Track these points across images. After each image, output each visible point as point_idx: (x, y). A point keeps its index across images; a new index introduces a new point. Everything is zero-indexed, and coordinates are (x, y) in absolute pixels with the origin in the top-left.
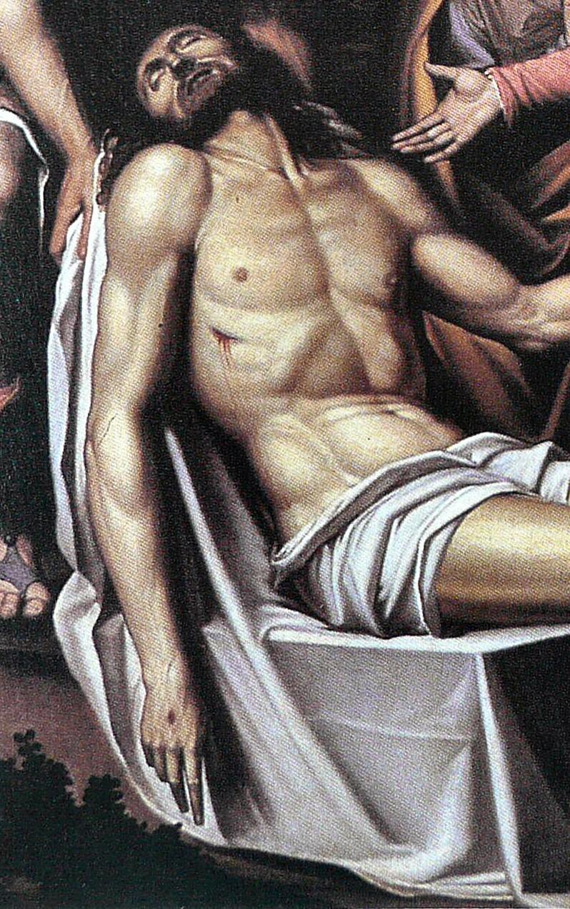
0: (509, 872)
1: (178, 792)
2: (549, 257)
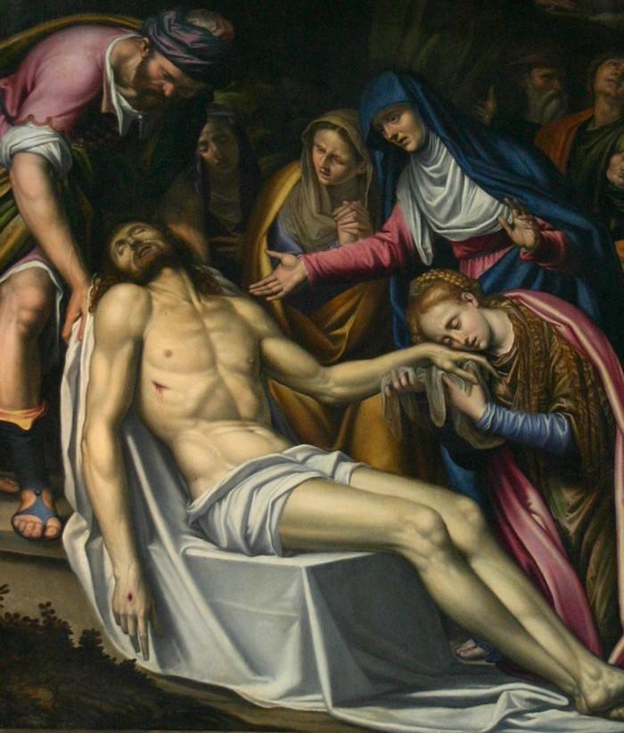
1: (134, 641)
2: (333, 354)
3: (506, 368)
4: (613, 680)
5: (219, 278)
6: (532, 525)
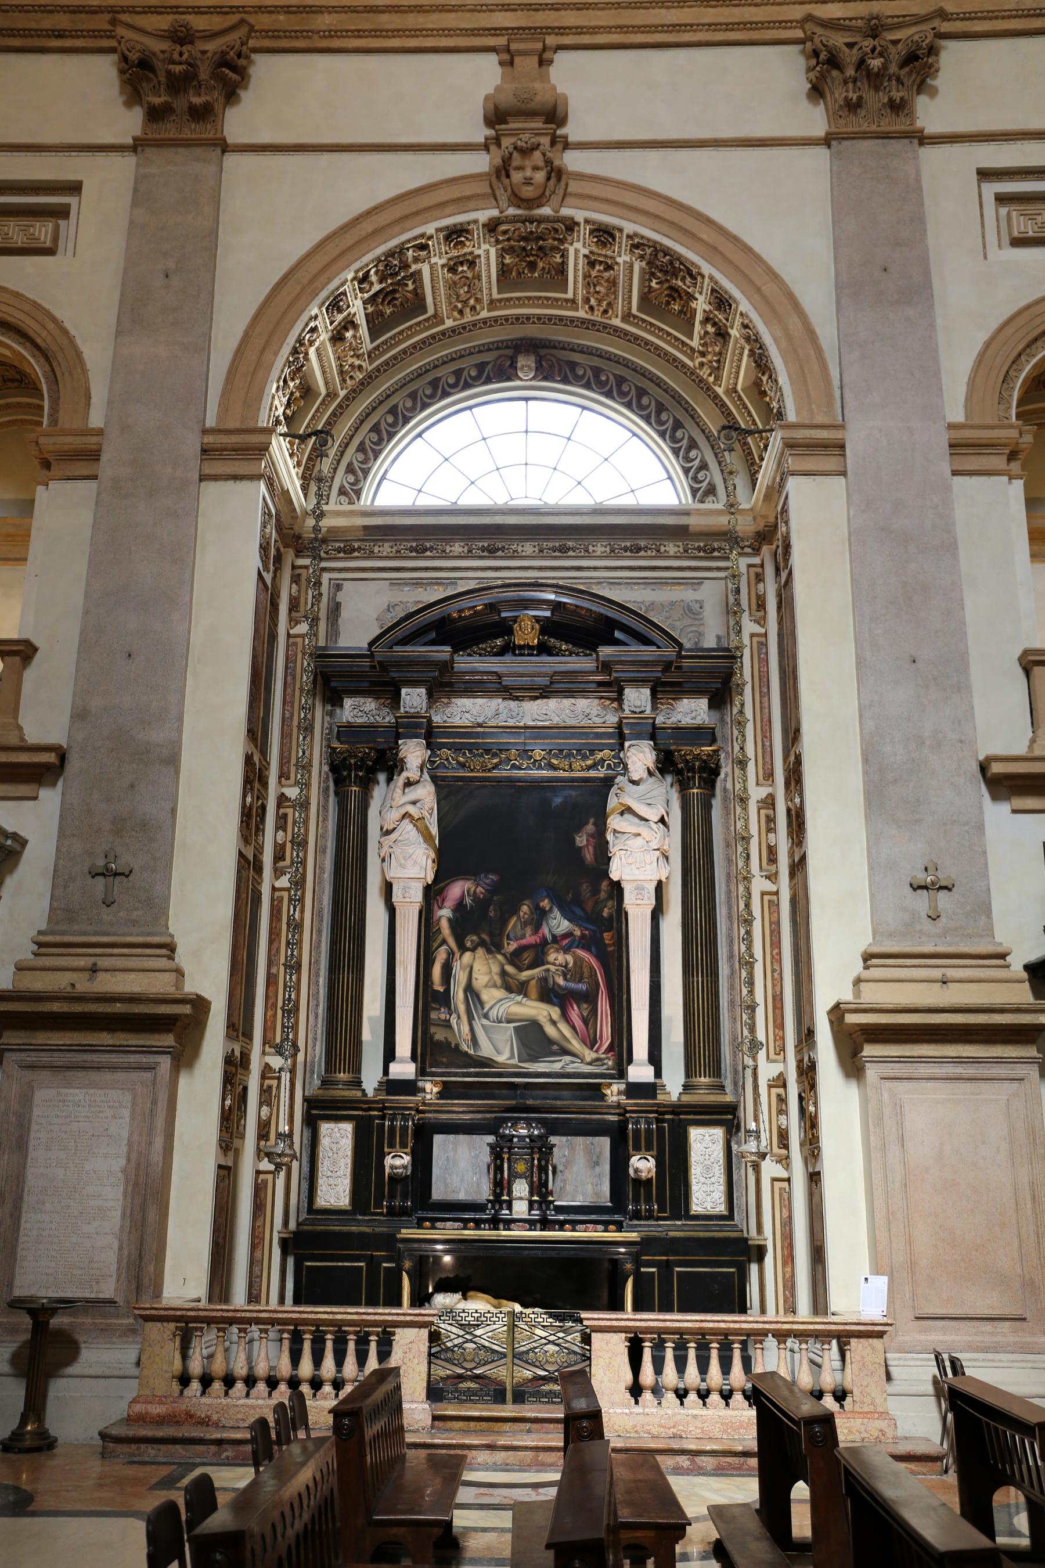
0: (515, 1061)
4: (594, 1055)
6: (574, 1014)
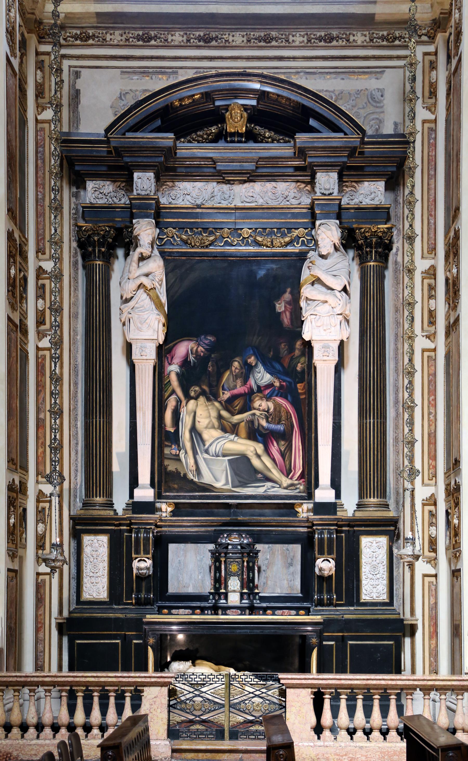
3: (271, 415)
5: (212, 397)
